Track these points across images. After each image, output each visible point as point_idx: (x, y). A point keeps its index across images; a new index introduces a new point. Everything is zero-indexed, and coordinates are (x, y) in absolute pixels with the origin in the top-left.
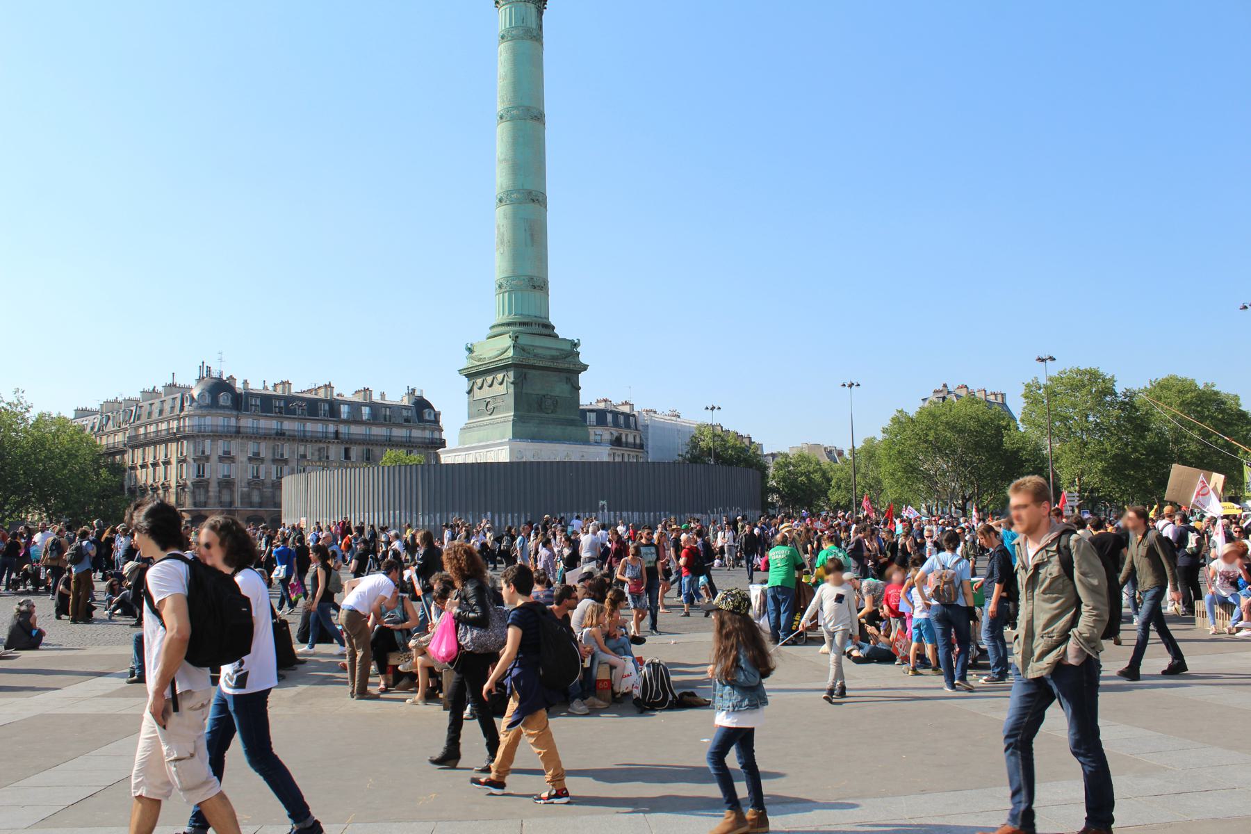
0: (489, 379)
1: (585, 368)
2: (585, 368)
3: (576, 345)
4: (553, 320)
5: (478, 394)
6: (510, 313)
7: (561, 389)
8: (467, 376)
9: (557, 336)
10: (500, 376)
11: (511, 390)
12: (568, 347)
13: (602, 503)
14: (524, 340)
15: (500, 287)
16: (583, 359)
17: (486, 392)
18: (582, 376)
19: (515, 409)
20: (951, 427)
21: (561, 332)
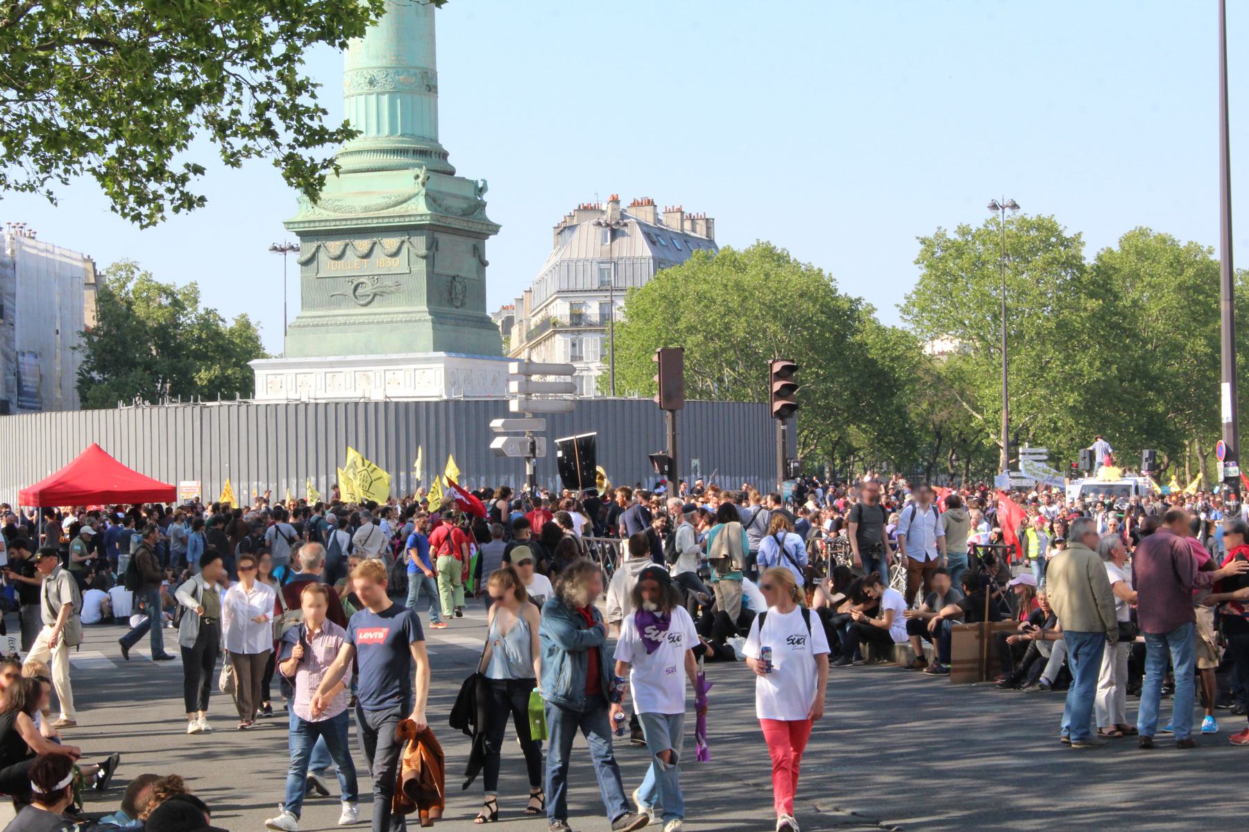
0: (363, 245)
1: (495, 229)
2: (495, 229)
3: (481, 191)
4: (445, 142)
5: (326, 266)
6: (393, 130)
7: (466, 267)
8: (298, 234)
9: (451, 173)
10: (391, 243)
11: (422, 266)
12: (470, 193)
13: (695, 462)
14: (432, 185)
15: (372, 82)
16: (491, 214)
17: (352, 265)
18: (492, 246)
19: (429, 302)
20: (773, 310)
21: (465, 165)
